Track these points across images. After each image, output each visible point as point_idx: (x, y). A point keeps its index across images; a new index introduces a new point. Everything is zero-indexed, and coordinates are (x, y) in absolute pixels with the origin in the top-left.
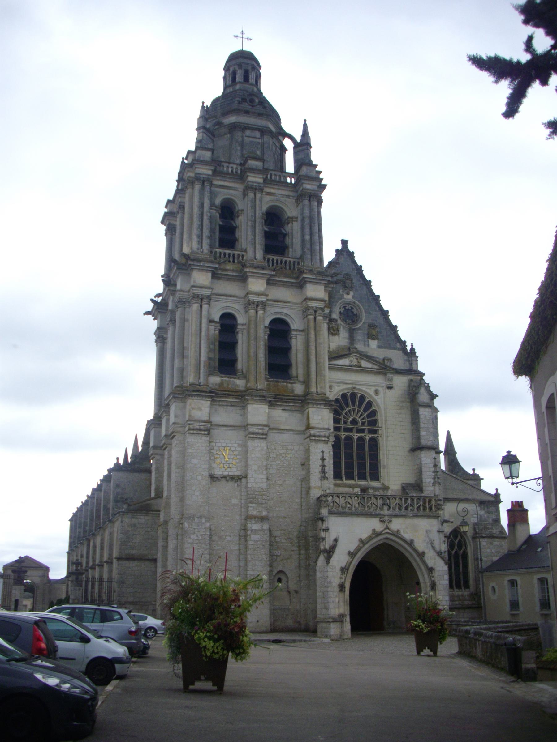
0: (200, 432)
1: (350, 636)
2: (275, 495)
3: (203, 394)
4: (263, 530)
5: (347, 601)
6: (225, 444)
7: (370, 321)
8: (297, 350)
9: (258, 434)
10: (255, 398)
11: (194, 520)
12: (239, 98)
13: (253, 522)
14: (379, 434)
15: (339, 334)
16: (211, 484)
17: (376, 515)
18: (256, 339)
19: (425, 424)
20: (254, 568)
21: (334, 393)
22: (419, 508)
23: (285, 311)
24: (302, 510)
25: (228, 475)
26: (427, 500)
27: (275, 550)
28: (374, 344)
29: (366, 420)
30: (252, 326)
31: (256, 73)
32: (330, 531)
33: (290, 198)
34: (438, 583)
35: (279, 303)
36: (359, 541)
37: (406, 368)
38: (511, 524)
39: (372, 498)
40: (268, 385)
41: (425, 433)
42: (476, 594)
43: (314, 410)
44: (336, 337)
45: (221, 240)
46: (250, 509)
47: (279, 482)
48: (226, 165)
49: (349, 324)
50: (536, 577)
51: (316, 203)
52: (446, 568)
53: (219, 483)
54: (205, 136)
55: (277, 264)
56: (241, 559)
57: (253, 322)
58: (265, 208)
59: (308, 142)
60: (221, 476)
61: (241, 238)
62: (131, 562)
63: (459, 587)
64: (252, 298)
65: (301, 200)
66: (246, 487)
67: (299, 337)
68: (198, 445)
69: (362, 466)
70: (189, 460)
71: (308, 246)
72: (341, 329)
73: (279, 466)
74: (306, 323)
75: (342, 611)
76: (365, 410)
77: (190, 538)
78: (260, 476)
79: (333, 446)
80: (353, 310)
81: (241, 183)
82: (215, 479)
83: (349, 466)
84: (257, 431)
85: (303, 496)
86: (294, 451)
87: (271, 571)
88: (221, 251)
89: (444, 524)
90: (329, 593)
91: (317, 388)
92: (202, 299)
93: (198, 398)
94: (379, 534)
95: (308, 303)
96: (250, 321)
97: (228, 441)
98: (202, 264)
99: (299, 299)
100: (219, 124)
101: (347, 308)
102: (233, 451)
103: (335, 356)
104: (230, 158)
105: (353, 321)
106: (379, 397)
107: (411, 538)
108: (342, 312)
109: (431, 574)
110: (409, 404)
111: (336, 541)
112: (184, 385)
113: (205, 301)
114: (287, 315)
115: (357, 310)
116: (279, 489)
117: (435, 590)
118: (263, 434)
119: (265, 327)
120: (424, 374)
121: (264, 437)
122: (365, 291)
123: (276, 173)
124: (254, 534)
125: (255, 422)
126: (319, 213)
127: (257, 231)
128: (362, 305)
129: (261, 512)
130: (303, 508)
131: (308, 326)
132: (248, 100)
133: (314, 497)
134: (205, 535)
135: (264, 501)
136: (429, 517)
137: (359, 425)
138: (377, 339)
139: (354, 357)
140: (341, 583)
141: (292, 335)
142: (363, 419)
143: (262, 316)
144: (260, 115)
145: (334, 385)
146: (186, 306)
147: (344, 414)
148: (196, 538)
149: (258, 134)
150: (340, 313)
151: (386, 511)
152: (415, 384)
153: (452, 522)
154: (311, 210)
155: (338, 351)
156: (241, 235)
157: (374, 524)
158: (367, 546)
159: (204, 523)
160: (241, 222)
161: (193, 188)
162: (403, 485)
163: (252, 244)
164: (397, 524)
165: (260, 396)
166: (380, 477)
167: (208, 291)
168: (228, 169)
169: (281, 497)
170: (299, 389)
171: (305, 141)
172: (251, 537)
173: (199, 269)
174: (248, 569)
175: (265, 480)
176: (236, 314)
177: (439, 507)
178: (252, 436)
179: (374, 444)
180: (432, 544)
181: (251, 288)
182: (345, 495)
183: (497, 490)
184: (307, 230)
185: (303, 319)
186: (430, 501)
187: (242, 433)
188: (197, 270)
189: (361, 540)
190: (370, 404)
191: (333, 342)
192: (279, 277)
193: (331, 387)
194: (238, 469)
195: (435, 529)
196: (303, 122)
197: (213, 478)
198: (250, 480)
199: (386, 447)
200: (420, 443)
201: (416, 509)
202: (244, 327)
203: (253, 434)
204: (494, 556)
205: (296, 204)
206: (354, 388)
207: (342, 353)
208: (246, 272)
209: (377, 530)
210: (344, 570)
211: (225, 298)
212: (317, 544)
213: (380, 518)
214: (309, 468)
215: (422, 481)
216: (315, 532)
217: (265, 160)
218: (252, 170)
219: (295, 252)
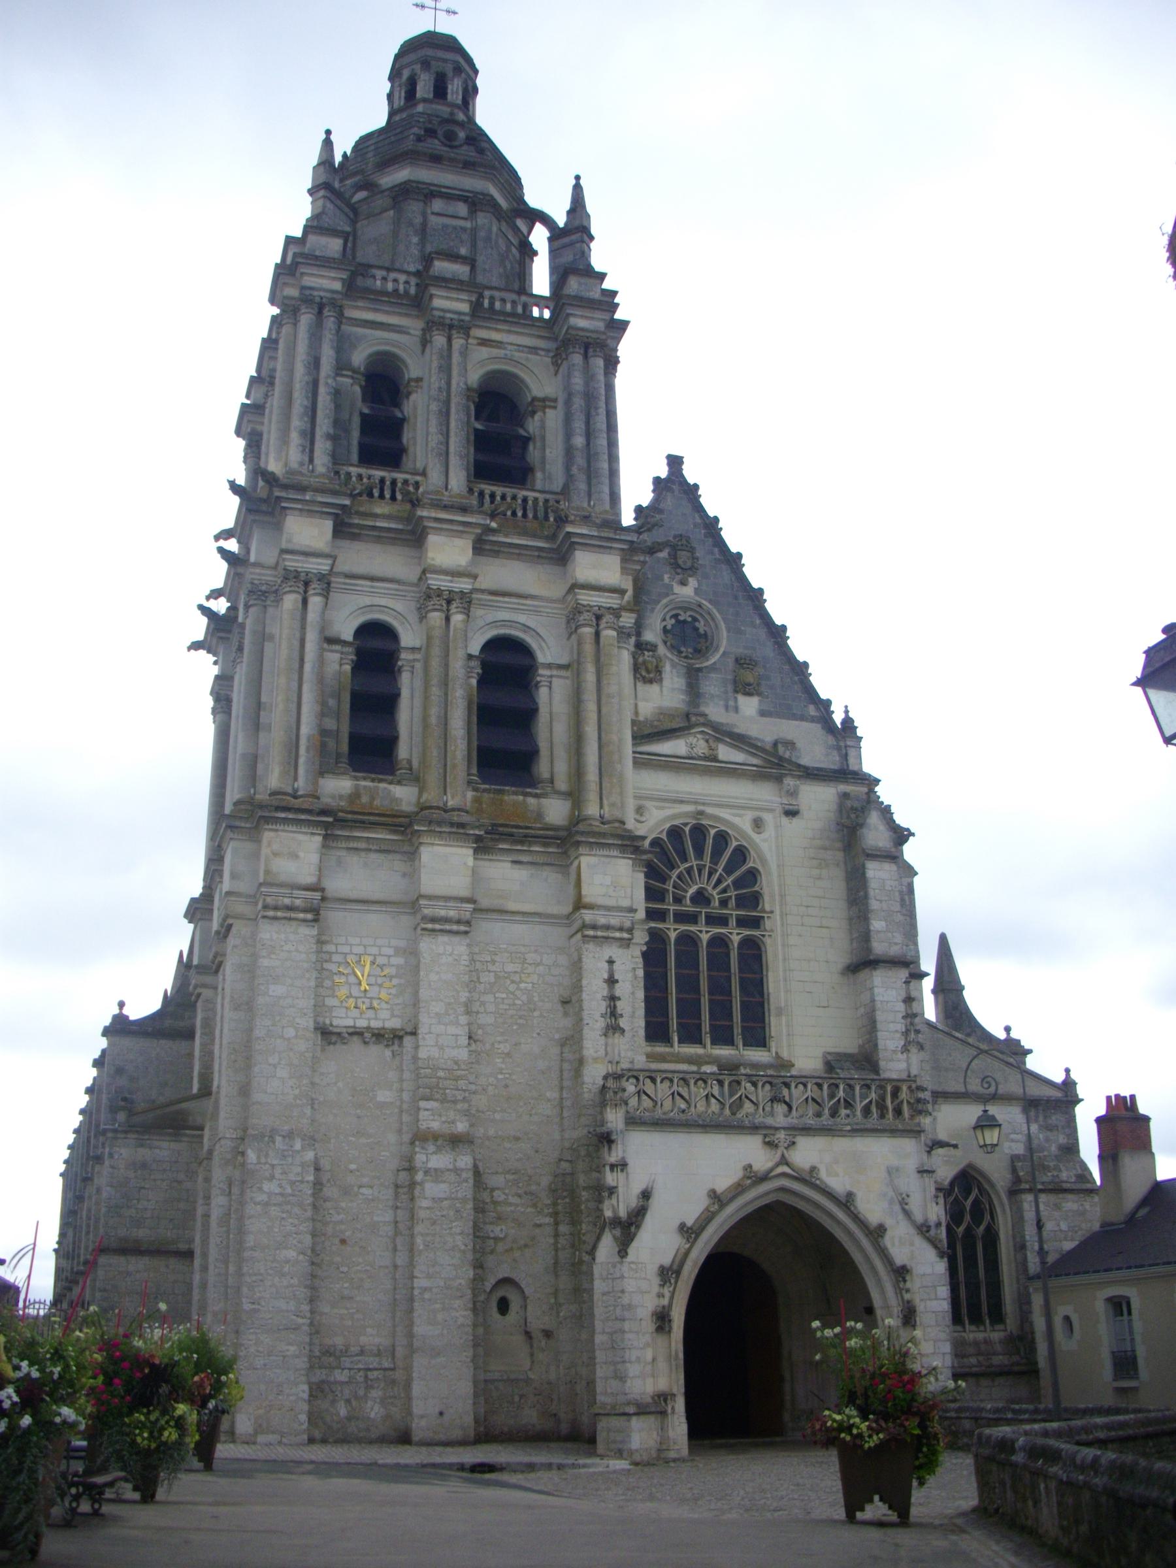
0: (293, 915)
1: (685, 1451)
2: (491, 1080)
3: (303, 817)
4: (456, 1171)
6: (362, 948)
7: (741, 650)
8: (551, 713)
9: (447, 920)
10: (438, 829)
11: (274, 1142)
12: (420, 128)
13: (431, 1148)
14: (765, 930)
15: (661, 680)
16: (323, 1050)
17: (754, 1129)
18: (445, 683)
19: (881, 901)
20: (431, 1271)
22: (867, 1111)
23: (522, 618)
24: (562, 1118)
25: (368, 1028)
26: (889, 1088)
27: (491, 1223)
28: (749, 706)
29: (732, 893)
30: (436, 651)
31: (465, 82)
32: (630, 1168)
33: (537, 354)
34: (920, 1307)
35: (506, 599)
36: (709, 1196)
37: (832, 767)
39: (743, 1083)
40: (477, 800)
41: (883, 923)
43: (593, 860)
44: (655, 688)
45: (363, 448)
46: (423, 1115)
47: (502, 1046)
48: (379, 273)
49: (686, 657)
51: (600, 363)
52: (941, 1267)
53: (345, 1047)
54: (329, 205)
56: (399, 1247)
57: (437, 642)
58: (474, 377)
59: (585, 224)
60: (351, 1030)
61: (415, 444)
63: (976, 1319)
64: (435, 581)
65: (564, 356)
66: (415, 1058)
67: (556, 682)
69: (721, 1010)
70: (263, 988)
71: (580, 461)
72: (667, 668)
73: (501, 1006)
74: (575, 647)
75: (663, 1384)
76: (729, 870)
77: (260, 1189)
78: (452, 1030)
79: (644, 955)
80: (697, 624)
81: (417, 317)
82: (334, 1039)
83: (689, 1009)
84: (443, 913)
85: (566, 1083)
86: (541, 968)
87: (477, 1280)
88: (363, 471)
89: (933, 1152)
90: (627, 1336)
91: (601, 807)
92: (307, 584)
93: (290, 828)
94: (764, 1178)
95: (578, 597)
96: (429, 638)
98: (308, 498)
99: (557, 590)
100: (369, 186)
101: (681, 618)
102: (382, 967)
103: (646, 733)
104: (393, 261)
105: (697, 651)
106: (762, 836)
107: (848, 1188)
108: (669, 627)
109: (901, 1285)
110: (840, 855)
111: (646, 1195)
112: (257, 796)
113: (315, 586)
114: (526, 628)
115: (707, 623)
116: (503, 1066)
118: (459, 922)
120: (877, 781)
121: (463, 928)
122: (726, 576)
124: (433, 1181)
125: (439, 891)
126: (610, 389)
127: (453, 424)
128: (718, 611)
129: (453, 1122)
130: (566, 1114)
132: (440, 133)
133: (594, 1084)
134: (302, 1182)
135: (459, 1095)
136: (893, 1132)
137: (715, 908)
138: (759, 694)
139: (698, 736)
140: (659, 1309)
141: (539, 679)
142: (724, 891)
144: (468, 165)
145: (649, 804)
146: (268, 603)
147: (674, 877)
148: (277, 1190)
149: (462, 209)
150: (665, 630)
151: (779, 1117)
152: (856, 804)
153: (955, 1146)
154: (589, 378)
155: (659, 721)
156: (414, 438)
158: (730, 1209)
159: (298, 1152)
160: (415, 408)
161: (295, 324)
162: (829, 1058)
163: (441, 454)
165: (452, 825)
166: (771, 1037)
167: (324, 564)
169: (506, 1086)
171: (577, 223)
172: (423, 1189)
173: (301, 510)
174: (416, 1273)
175: (464, 1040)
176: (395, 624)
177: (920, 1107)
178: (430, 926)
179: (753, 953)
181: (433, 559)
182: (670, 1075)
183: (1067, 1071)
184: (579, 425)
185: (569, 638)
186: (896, 1093)
187: (406, 921)
188: (297, 513)
189: (713, 1195)
190: (741, 854)
191: (647, 701)
192: (506, 536)
193: (640, 810)
194: (396, 1013)
196: (574, 182)
198: (424, 1039)
199: (784, 960)
200: (869, 950)
201: (858, 1113)
202: (417, 656)
203: (433, 920)
204: (1066, 1239)
205: (552, 369)
206: (701, 813)
207: (668, 725)
208: (421, 518)
209: (755, 1168)
210: (668, 1274)
211: (368, 583)
213: (765, 1136)
214: (581, 1009)
215: (876, 1045)
216: (595, 1175)
218: (445, 282)
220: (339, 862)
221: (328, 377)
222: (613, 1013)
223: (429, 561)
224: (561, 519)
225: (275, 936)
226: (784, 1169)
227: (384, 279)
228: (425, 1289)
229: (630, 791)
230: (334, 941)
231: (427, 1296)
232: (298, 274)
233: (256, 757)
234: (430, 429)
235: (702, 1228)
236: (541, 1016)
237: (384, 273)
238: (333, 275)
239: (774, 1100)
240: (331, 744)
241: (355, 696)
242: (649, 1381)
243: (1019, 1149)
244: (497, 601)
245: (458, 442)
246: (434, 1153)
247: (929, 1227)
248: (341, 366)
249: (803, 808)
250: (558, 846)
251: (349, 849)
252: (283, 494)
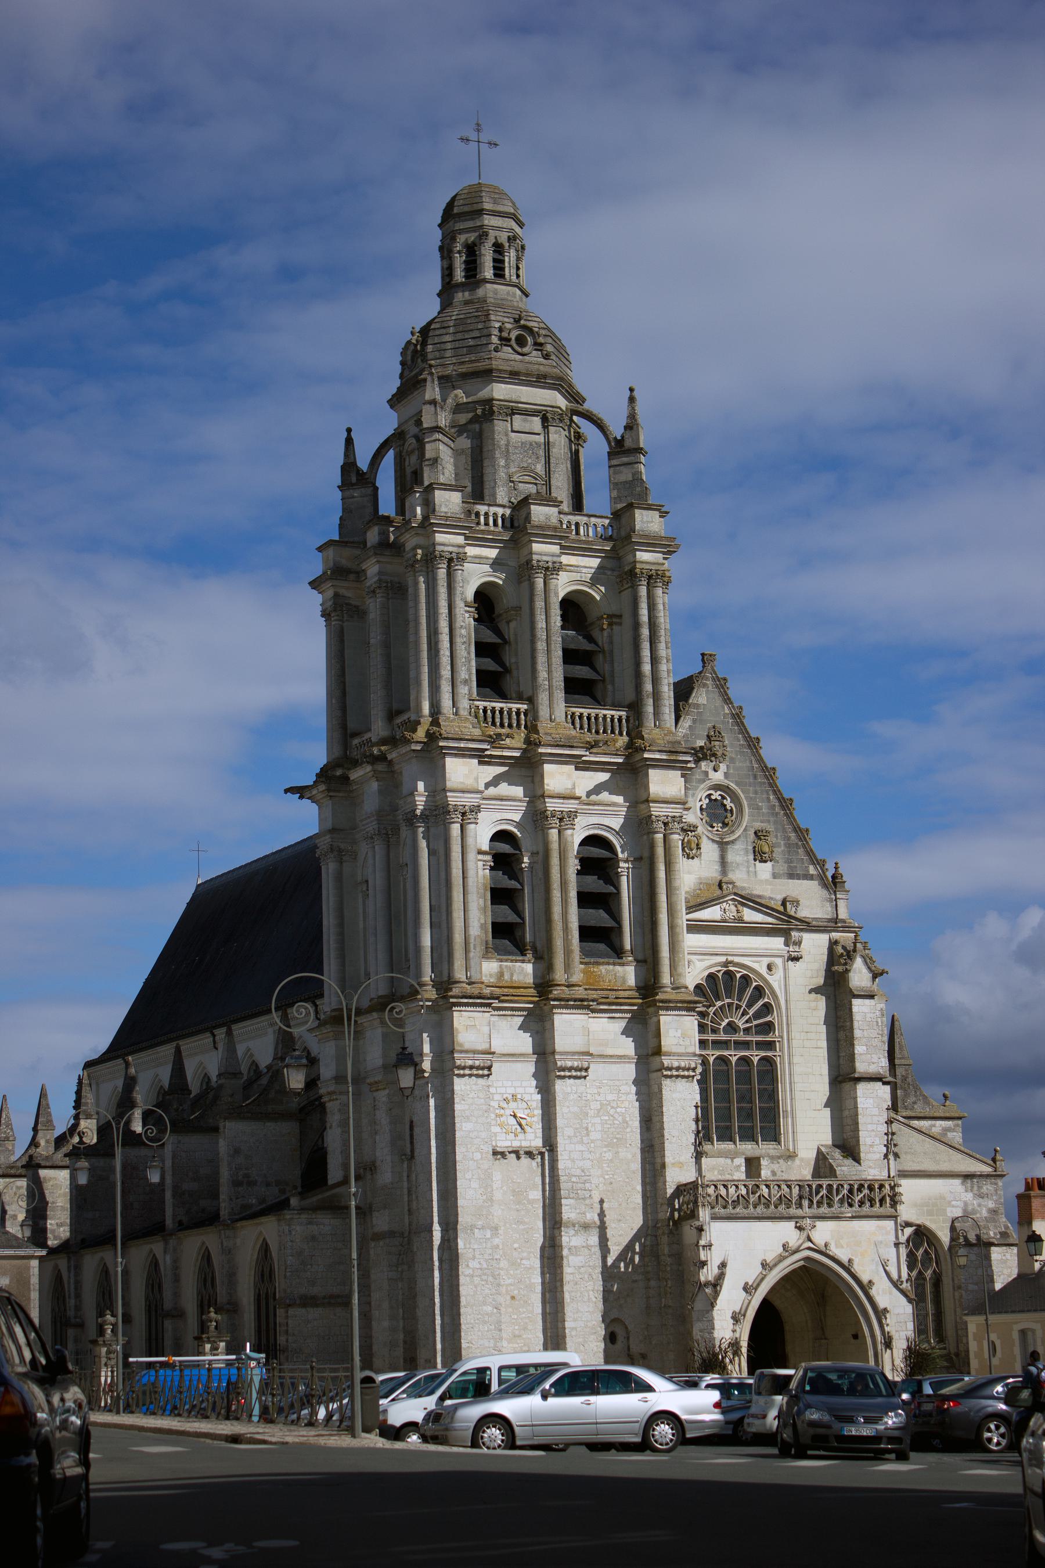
4: (588, 1247)
9: (570, 1069)
13: (572, 1232)
17: (789, 1218)
21: (694, 974)
25: (521, 1147)
28: (765, 870)
36: (762, 1264)
37: (826, 917)
41: (865, 1048)
52: (908, 1309)
53: (505, 1161)
62: (311, 1310)
69: (748, 1115)
77: (468, 1266)
79: (697, 1080)
82: (499, 1156)
84: (569, 1064)
92: (464, 814)
95: (652, 809)
97: (518, 1084)
101: (713, 797)
107: (850, 1257)
111: (723, 1265)
118: (580, 1070)
121: (584, 1074)
129: (584, 1213)
134: (492, 1259)
137: (741, 1037)
142: (747, 1022)
144: (540, 380)
148: (478, 1266)
149: (536, 423)
150: (701, 809)
151: (806, 1210)
157: (785, 1232)
164: (824, 1232)
165: (575, 1000)
178: (562, 1073)
186: (881, 1186)
190: (759, 992)
191: (689, 873)
197: (495, 1153)
198: (561, 1155)
203: (563, 1069)
206: (731, 962)
211: (499, 803)
212: (680, 1268)
213: (797, 1222)
215: (858, 1141)
223: (546, 787)
225: (463, 1088)
228: (573, 1329)
229: (686, 960)
230: (495, 1085)
231: (574, 1333)
235: (758, 1285)
236: (632, 1131)
241: (492, 890)
243: (958, 1213)
244: (589, 809)
246: (574, 1235)
247: (902, 1282)
249: (804, 953)
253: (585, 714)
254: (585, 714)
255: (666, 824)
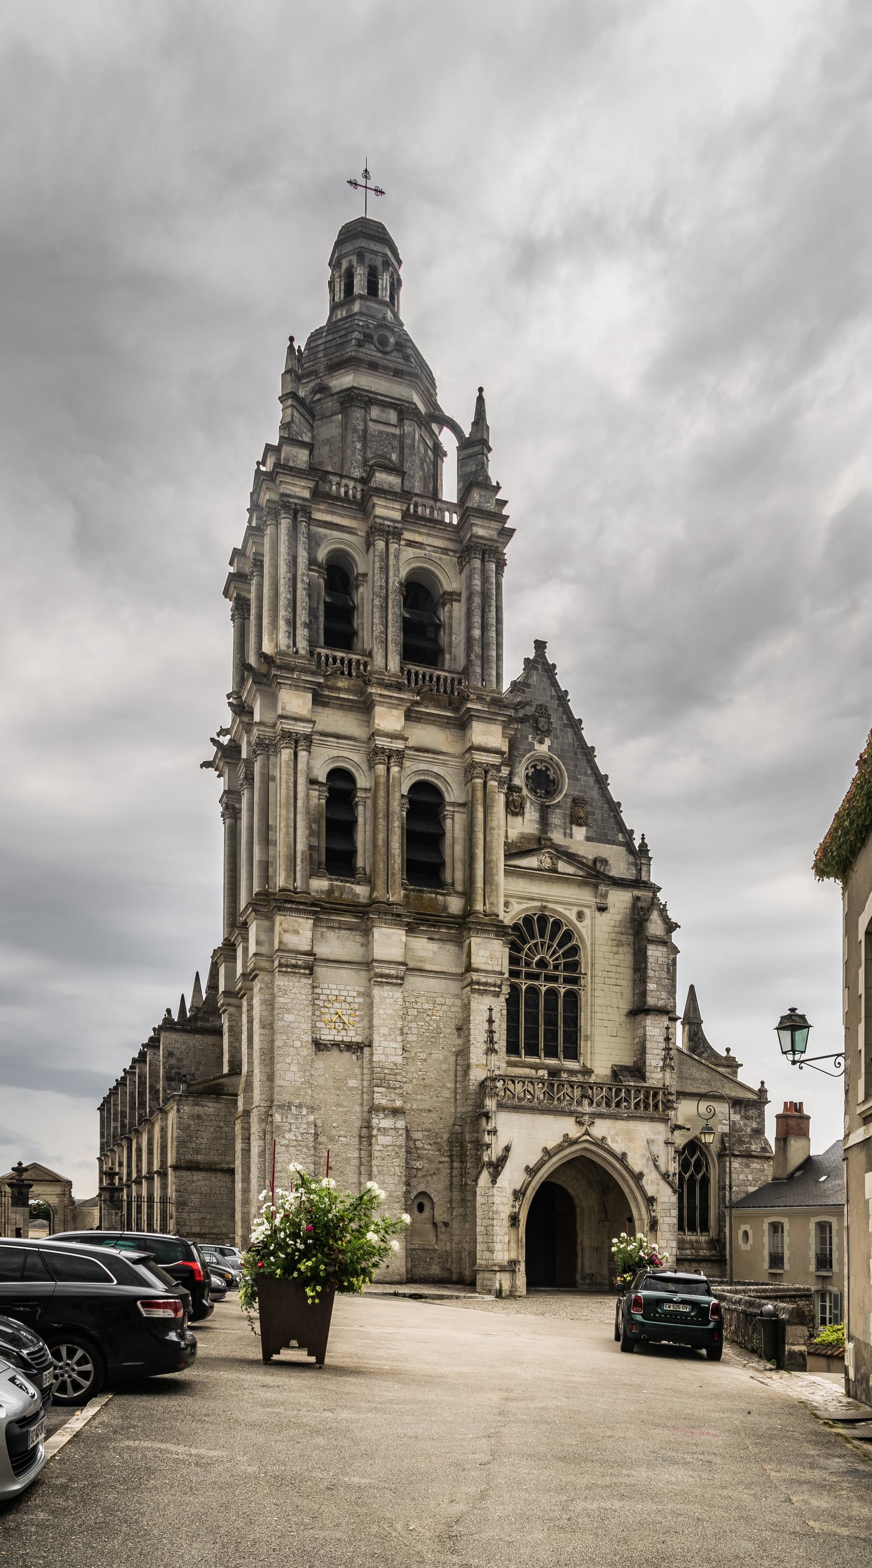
1: (524, 1293)
4: (395, 1129)
5: (521, 1241)
8: (453, 838)
13: (382, 1116)
16: (316, 1054)
17: (571, 1114)
18: (388, 816)
22: (637, 1105)
23: (436, 769)
25: (342, 1041)
30: (382, 793)
34: (660, 1221)
35: (426, 755)
38: (783, 1139)
40: (406, 896)
42: (718, 1241)
43: (478, 940)
50: (814, 1220)
52: (674, 1199)
55: (424, 682)
57: (382, 787)
58: (403, 573)
61: (363, 629)
63: (692, 1229)
66: (371, 1061)
68: (293, 991)
74: (470, 792)
78: (393, 1045)
84: (387, 971)
87: (407, 1193)
89: (675, 1132)
90: (495, 1228)
91: (484, 905)
94: (575, 1142)
104: (342, 467)
107: (624, 1150)
114: (438, 776)
117: (656, 1231)
118: (397, 978)
119: (403, 796)
121: (399, 981)
123: (425, 501)
131: (473, 797)
135: (397, 1085)
136: (652, 1119)
143: (397, 775)
149: (393, 416)
151: (586, 1108)
153: (688, 1129)
156: (362, 624)
157: (567, 1127)
160: (362, 599)
164: (601, 1129)
168: (338, 490)
170: (455, 905)
171: (479, 436)
175: (400, 1051)
178: (379, 979)
179: (573, 999)
180: (655, 1161)
185: (466, 784)
186: (655, 1095)
187: (363, 974)
192: (426, 707)
195: (661, 1138)
197: (319, 1045)
199: (592, 1005)
201: (632, 1107)
202: (368, 795)
203: (382, 976)
213: (577, 1118)
214: (469, 1034)
217: (405, 473)
219: (455, 659)
220: (322, 935)
221: (303, 575)
222: (491, 1041)
224: (464, 697)
226: (587, 1137)
227: (338, 484)
229: (502, 892)
232: (277, 482)
233: (267, 863)
234: (375, 620)
237: (338, 479)
238: (303, 484)
239: (583, 1096)
240: (315, 855)
241: (328, 820)
242: (506, 1253)
245: (394, 632)
248: (312, 562)
250: (457, 929)
251: (328, 927)
252: (279, 673)
253: (421, 672)
254: (421, 672)
255: (486, 772)
